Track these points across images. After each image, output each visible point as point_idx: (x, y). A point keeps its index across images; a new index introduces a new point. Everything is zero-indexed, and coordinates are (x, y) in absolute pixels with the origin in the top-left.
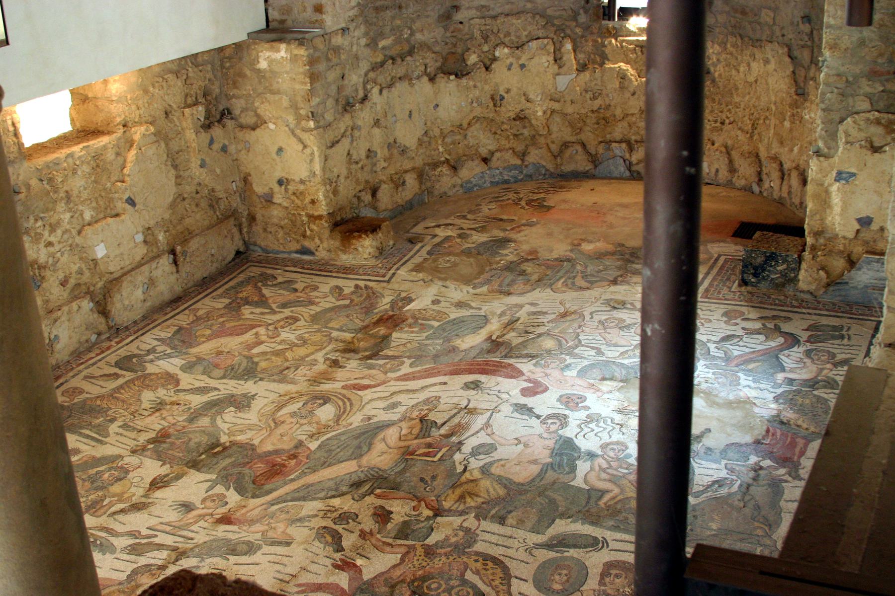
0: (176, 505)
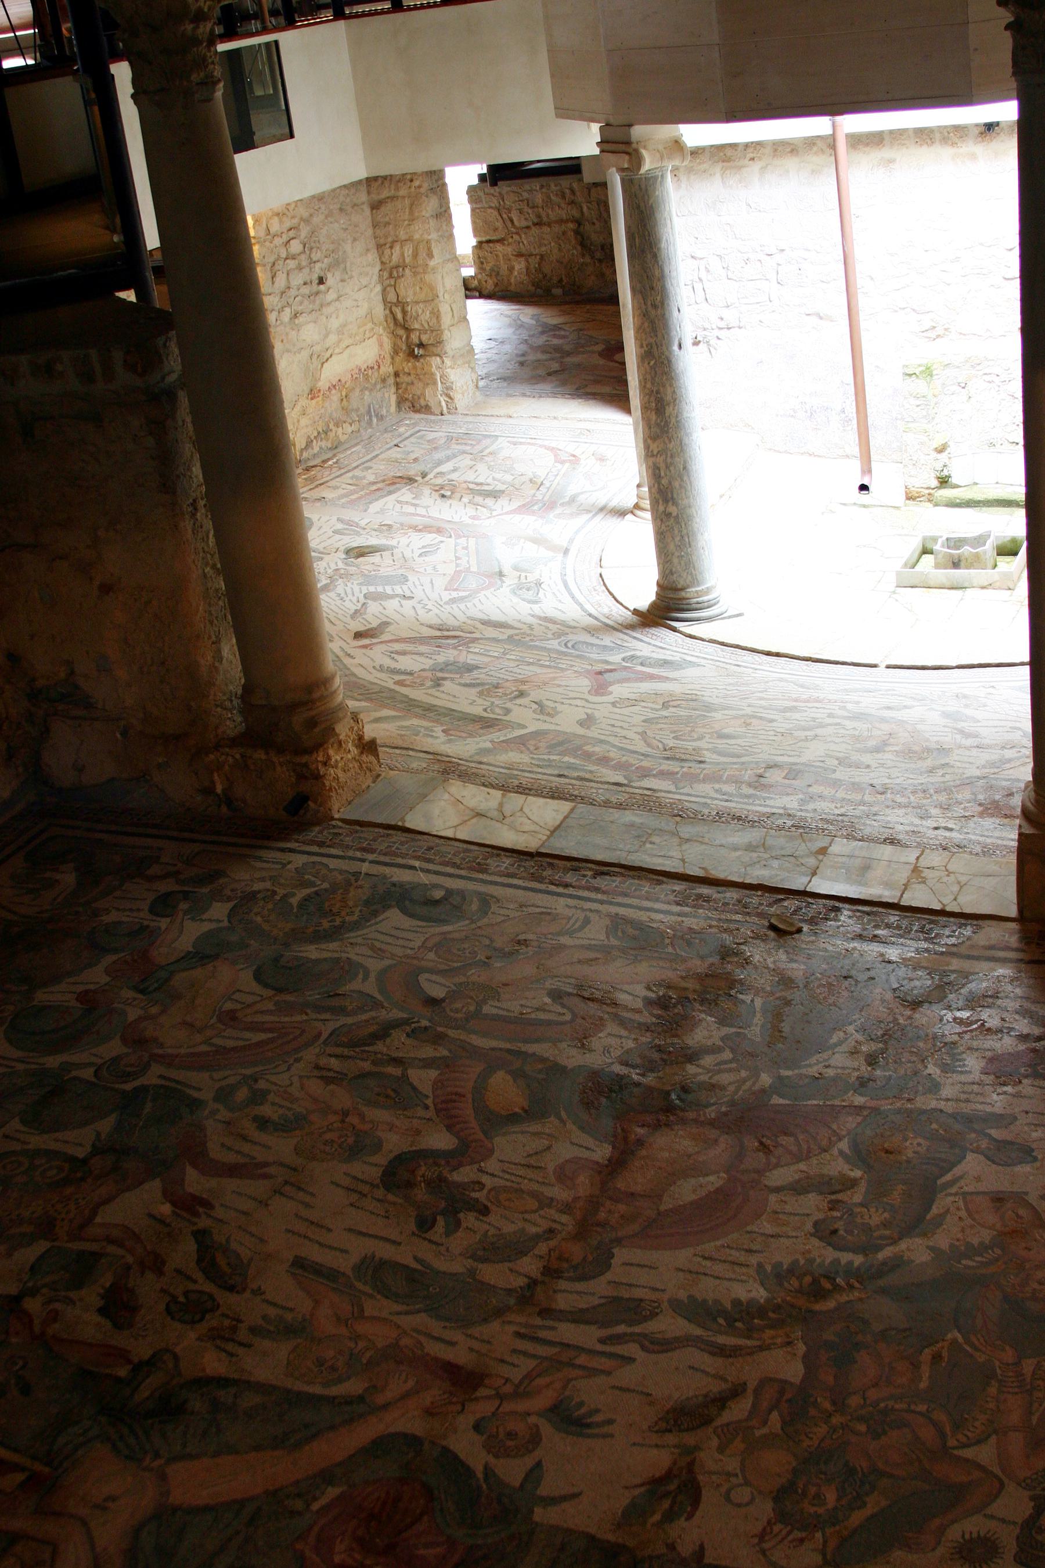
0: (598, 1425)
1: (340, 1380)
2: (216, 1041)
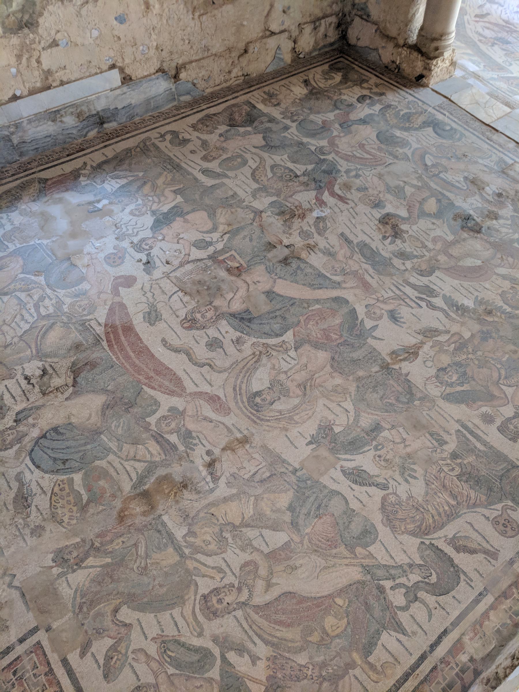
0: (401, 322)
1: (336, 275)
2: (355, 153)
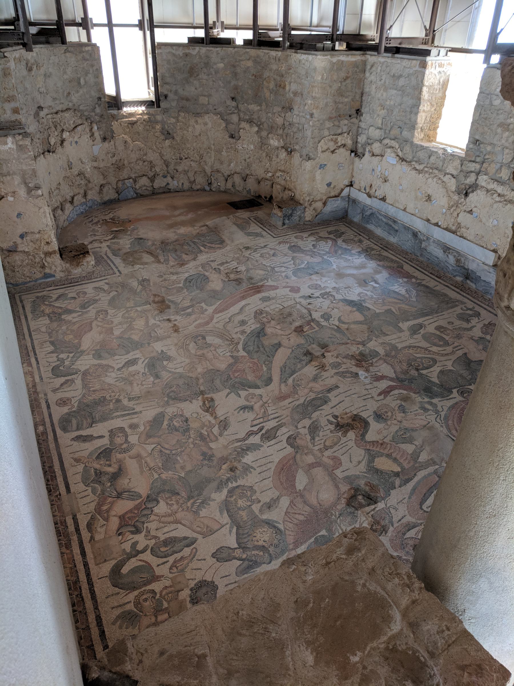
1: (294, 381)
